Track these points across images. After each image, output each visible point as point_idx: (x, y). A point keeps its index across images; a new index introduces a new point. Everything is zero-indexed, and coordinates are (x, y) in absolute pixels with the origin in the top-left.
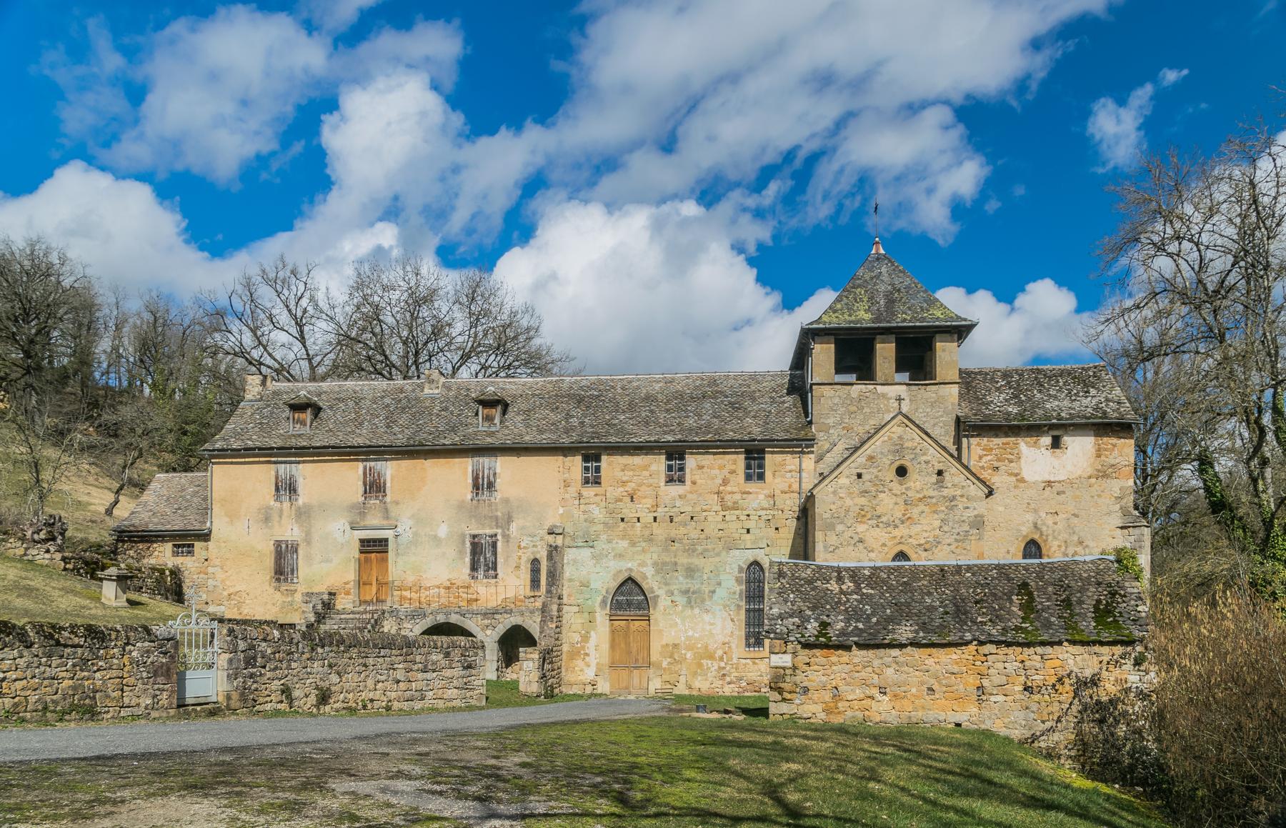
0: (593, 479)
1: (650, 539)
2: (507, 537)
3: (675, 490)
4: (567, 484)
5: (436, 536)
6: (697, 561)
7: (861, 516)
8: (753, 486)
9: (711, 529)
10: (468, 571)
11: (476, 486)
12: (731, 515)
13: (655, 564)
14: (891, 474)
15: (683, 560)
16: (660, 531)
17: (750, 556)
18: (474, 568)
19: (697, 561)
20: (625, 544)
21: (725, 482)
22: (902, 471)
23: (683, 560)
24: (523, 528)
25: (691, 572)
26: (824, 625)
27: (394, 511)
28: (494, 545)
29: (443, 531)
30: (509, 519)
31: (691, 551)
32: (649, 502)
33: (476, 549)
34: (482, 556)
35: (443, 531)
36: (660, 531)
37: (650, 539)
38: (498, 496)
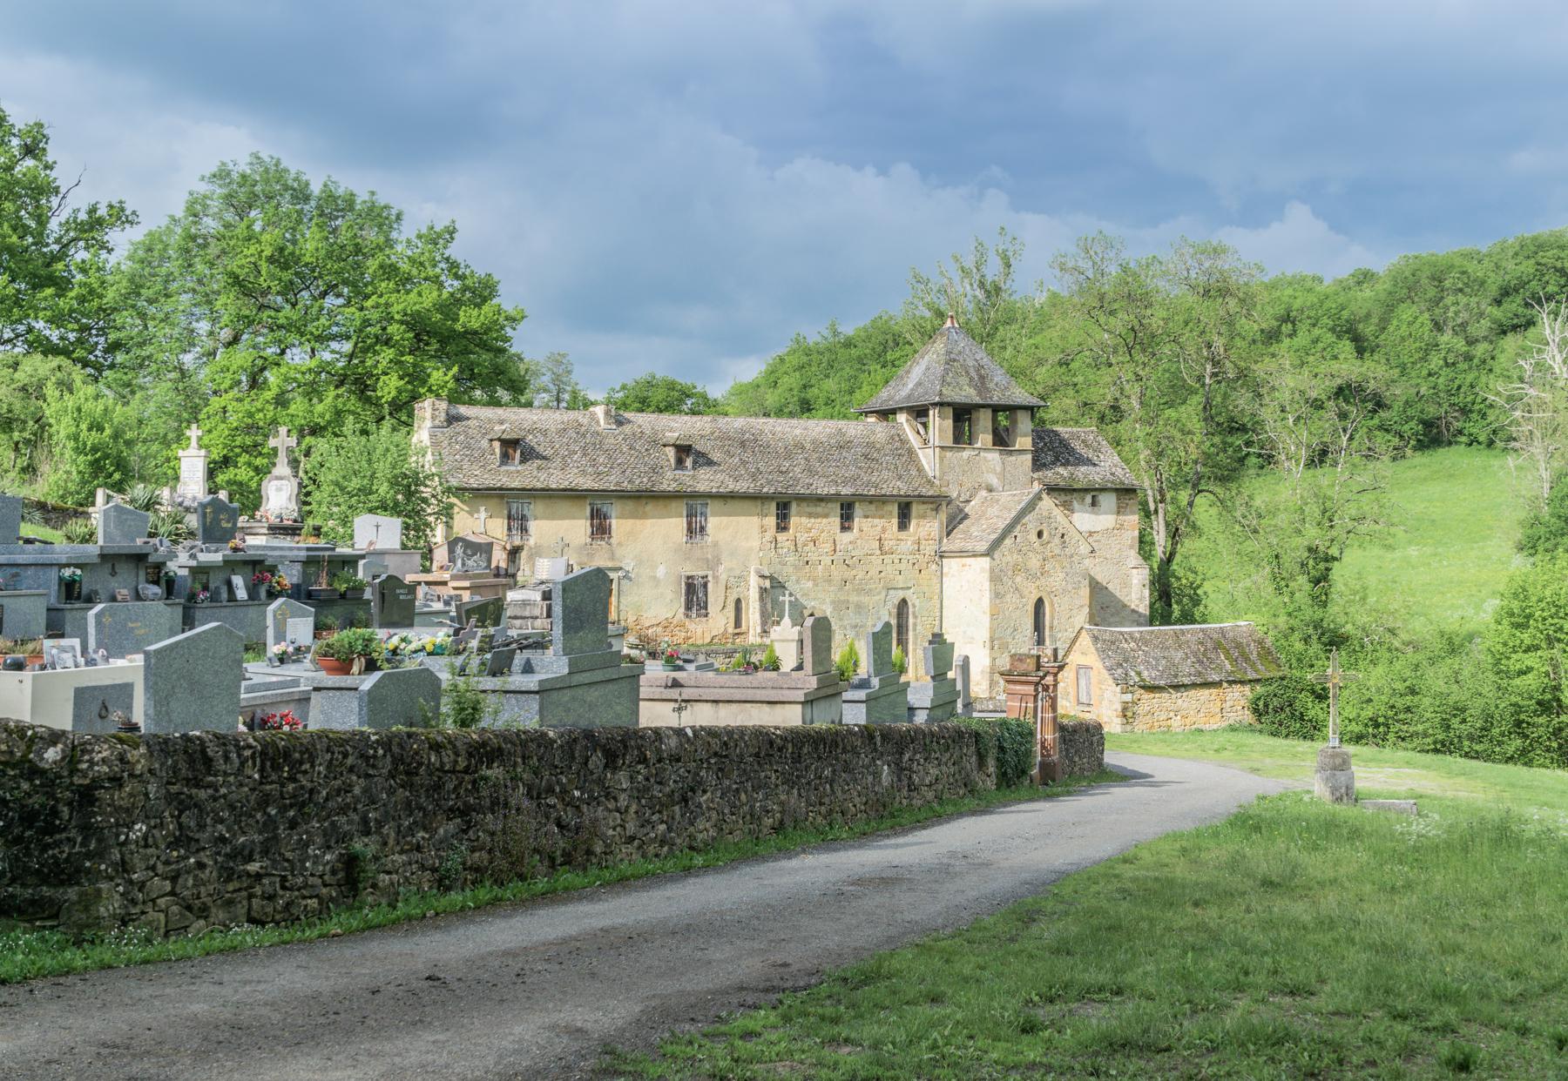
0: (782, 527)
1: (829, 580)
2: (716, 578)
3: (847, 537)
4: (763, 530)
5: (655, 577)
6: (865, 599)
7: (1016, 569)
8: (903, 535)
9: (873, 572)
10: (682, 610)
11: (690, 531)
12: (888, 559)
13: (833, 602)
14: (1034, 537)
15: (854, 598)
16: (838, 572)
17: (901, 594)
18: (688, 608)
19: (865, 599)
20: (810, 584)
21: (884, 530)
22: (1040, 534)
23: (854, 598)
24: (731, 570)
25: (859, 607)
26: (1139, 674)
27: (619, 552)
28: (705, 585)
29: (661, 572)
30: (719, 562)
31: (860, 591)
32: (828, 547)
33: (691, 588)
34: (695, 595)
35: (661, 572)
36: (838, 572)
37: (829, 580)
38: (709, 539)
